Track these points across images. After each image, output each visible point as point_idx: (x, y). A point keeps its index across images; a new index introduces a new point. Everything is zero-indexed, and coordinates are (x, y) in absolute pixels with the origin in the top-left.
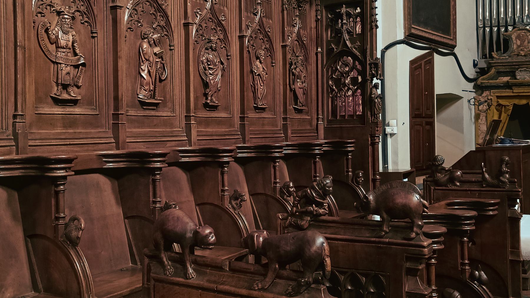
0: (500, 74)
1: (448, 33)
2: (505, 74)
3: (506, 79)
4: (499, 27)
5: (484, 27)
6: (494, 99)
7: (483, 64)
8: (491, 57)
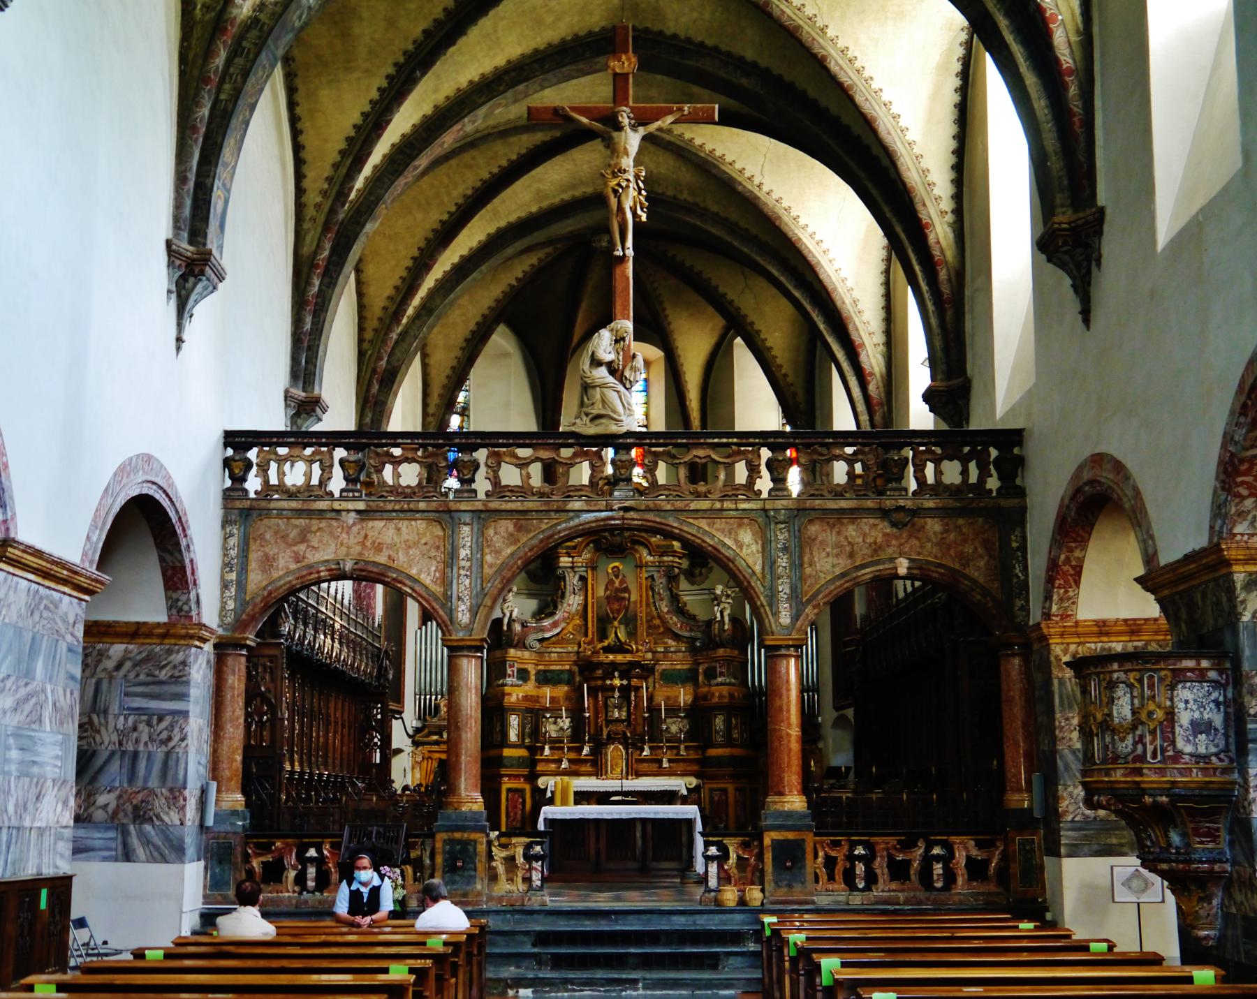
0: (431, 733)
1: (399, 703)
2: (435, 734)
3: (435, 737)
4: (431, 695)
5: (420, 695)
6: (425, 752)
7: (419, 724)
8: (425, 720)
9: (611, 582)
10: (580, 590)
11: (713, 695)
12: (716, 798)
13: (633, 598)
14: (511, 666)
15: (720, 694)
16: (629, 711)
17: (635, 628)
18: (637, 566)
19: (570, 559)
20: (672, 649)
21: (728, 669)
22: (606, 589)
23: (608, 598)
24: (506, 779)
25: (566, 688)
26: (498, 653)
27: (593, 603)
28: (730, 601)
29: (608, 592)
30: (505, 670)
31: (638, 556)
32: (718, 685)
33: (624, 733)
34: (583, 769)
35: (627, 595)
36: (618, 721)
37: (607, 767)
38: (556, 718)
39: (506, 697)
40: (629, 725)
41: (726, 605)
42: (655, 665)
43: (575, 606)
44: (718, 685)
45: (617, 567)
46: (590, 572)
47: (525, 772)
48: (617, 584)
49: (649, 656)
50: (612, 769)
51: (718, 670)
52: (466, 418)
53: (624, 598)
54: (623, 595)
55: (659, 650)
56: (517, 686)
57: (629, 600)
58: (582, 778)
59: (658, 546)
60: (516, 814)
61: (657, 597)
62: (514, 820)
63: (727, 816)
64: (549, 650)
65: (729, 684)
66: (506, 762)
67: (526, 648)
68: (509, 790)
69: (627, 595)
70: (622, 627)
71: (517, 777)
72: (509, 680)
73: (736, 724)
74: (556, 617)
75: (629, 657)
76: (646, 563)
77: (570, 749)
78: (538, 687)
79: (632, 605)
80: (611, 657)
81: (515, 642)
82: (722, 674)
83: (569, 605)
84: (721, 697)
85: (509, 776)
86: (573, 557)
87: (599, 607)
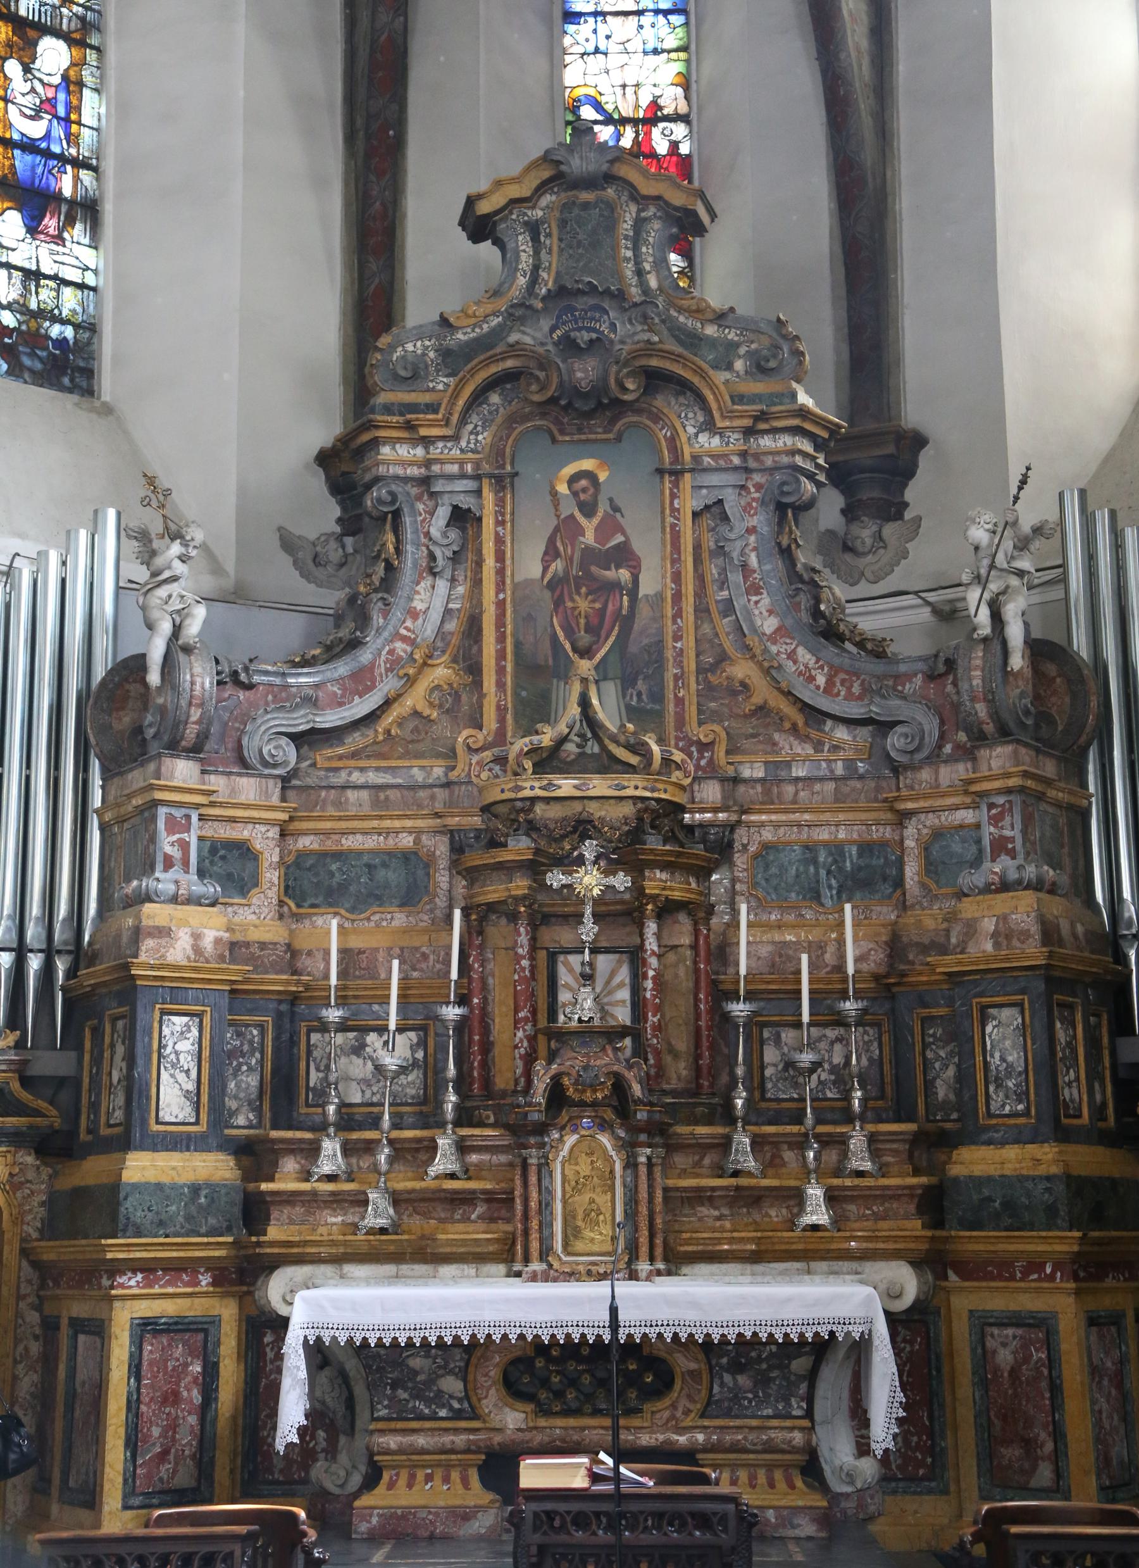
9: (567, 528)
10: (456, 558)
11: (971, 929)
12: (1005, 1357)
13: (647, 587)
14: (173, 826)
15: (1003, 918)
16: (638, 1005)
17: (658, 696)
18: (660, 472)
19: (419, 452)
20: (799, 771)
21: (1027, 821)
22: (551, 553)
23: (552, 585)
24: (132, 1282)
25: (400, 919)
26: (136, 778)
27: (501, 605)
28: (1025, 564)
29: (558, 566)
30: (153, 839)
31: (663, 434)
32: (987, 889)
33: (619, 1087)
34: (453, 1234)
35: (624, 575)
36: (586, 1033)
37: (546, 1225)
38: (365, 1030)
39: (148, 944)
40: (640, 1050)
41: (1014, 581)
42: (732, 827)
43: (435, 616)
44: (987, 889)
45: (590, 475)
46: (489, 497)
47: (218, 1246)
48: (589, 538)
49: (711, 792)
50: (572, 1233)
51: (988, 831)
52: (91, 56)
53: (616, 586)
54: (610, 574)
55: (746, 773)
56: (193, 900)
57: (633, 592)
58: (447, 1270)
59: (737, 398)
60: (173, 1426)
61: (736, 577)
62: (163, 1455)
63: (1058, 1434)
64: (341, 778)
65: (1037, 886)
66: (130, 1207)
67: (243, 762)
68: (145, 1328)
69: (624, 575)
70: (611, 688)
71: (176, 1268)
72: (164, 881)
73: (1071, 1045)
74: (365, 656)
75: (635, 786)
76: (696, 458)
77: (400, 1151)
78: (297, 917)
79: (644, 612)
80: (566, 785)
81: (191, 732)
82: (1001, 846)
83: (414, 614)
84: (1004, 935)
85: (147, 1268)
86: (427, 441)
87: (526, 620)
